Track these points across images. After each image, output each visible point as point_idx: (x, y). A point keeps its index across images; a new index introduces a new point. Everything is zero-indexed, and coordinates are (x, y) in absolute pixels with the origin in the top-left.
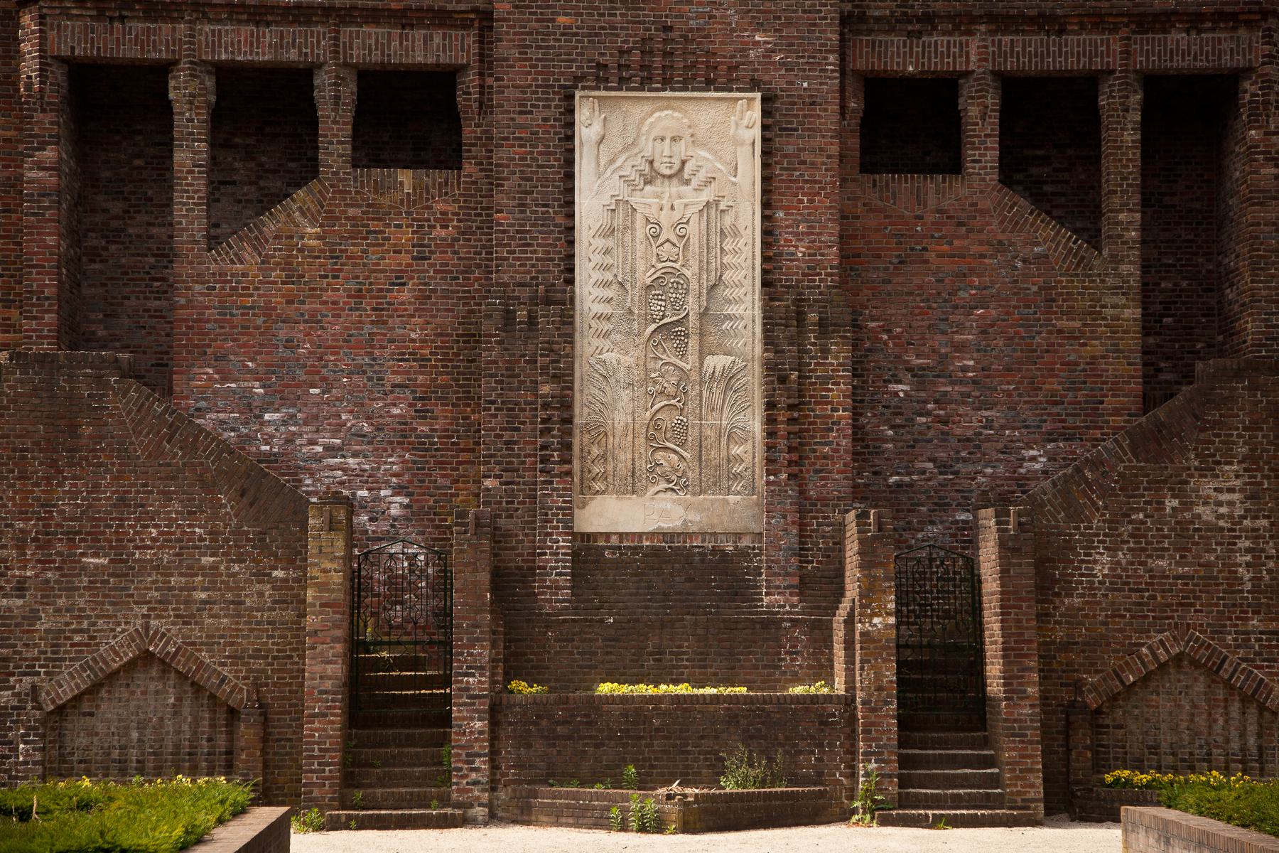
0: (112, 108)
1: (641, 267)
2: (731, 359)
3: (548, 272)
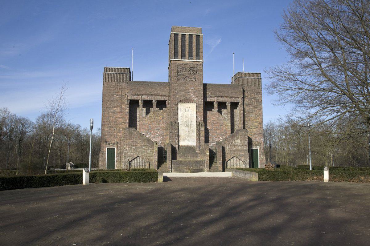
0: (133, 104)
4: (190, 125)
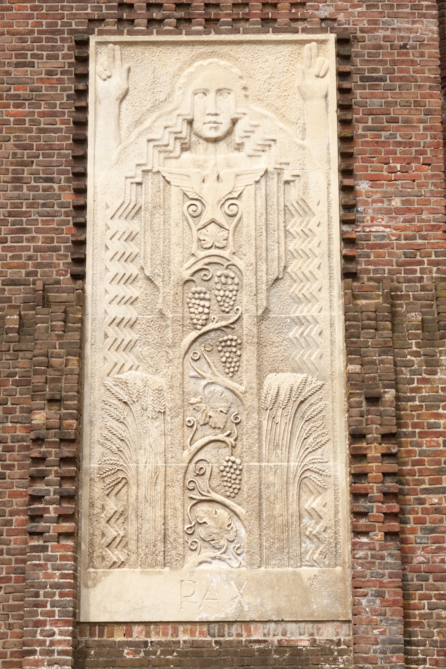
1: (176, 255)
2: (301, 377)
3: (49, 265)
4: (248, 325)
